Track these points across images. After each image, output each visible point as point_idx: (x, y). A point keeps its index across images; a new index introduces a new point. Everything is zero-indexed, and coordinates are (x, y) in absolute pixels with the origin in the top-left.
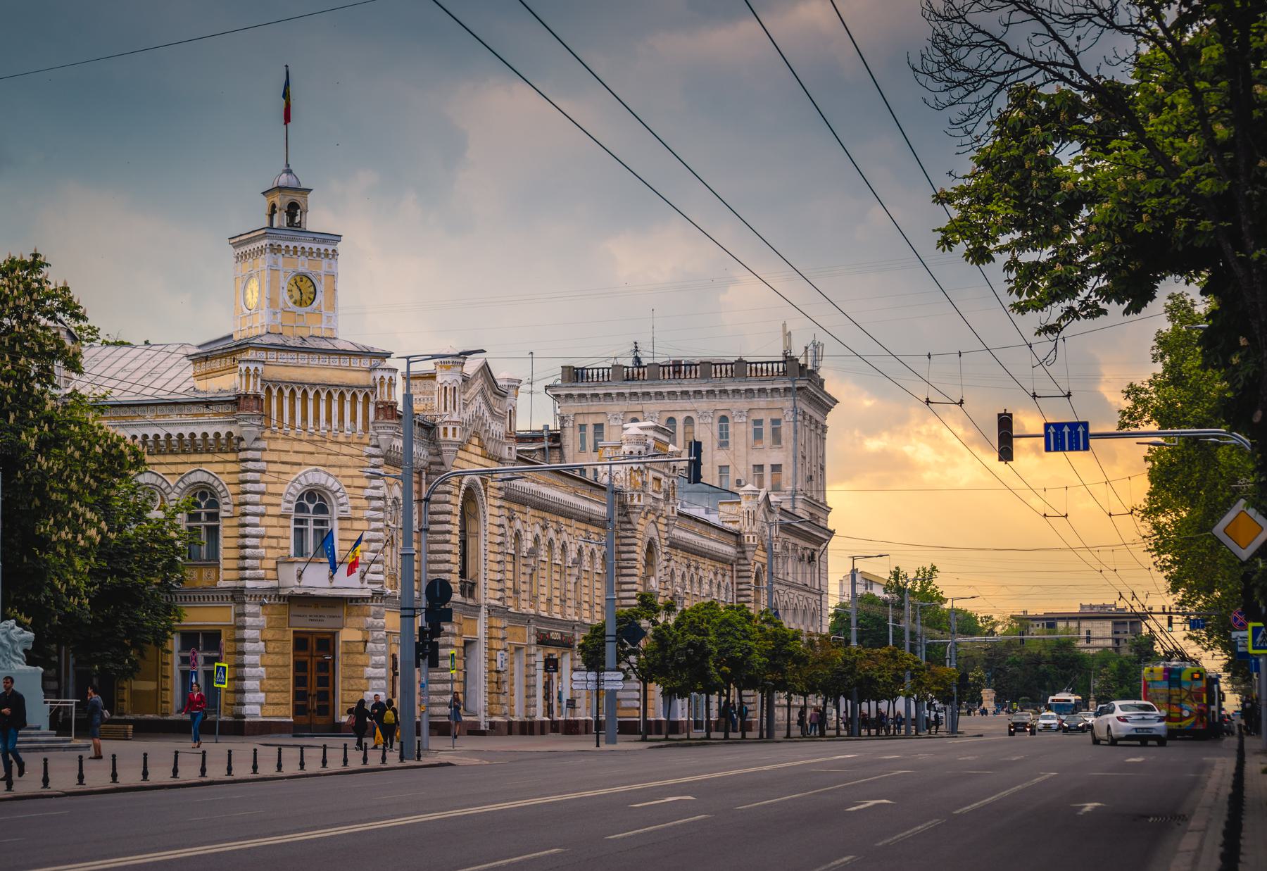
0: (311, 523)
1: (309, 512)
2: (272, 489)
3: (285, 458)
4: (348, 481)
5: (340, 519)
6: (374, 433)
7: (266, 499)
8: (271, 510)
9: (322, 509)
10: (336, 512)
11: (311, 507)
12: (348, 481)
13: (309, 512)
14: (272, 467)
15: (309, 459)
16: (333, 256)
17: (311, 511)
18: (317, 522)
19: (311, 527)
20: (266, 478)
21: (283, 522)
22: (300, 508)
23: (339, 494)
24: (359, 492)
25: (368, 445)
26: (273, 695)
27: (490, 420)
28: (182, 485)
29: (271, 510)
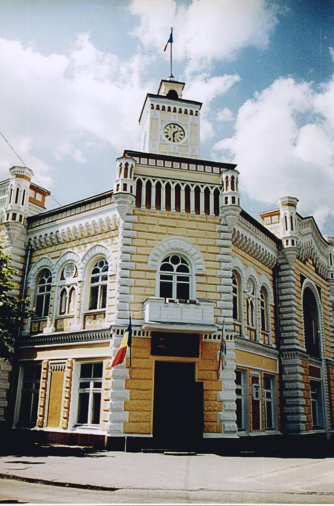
0: (175, 278)
1: (173, 270)
2: (140, 250)
3: (151, 229)
4: (204, 248)
5: (197, 275)
6: (223, 215)
7: (135, 258)
8: (139, 266)
9: (183, 269)
10: (193, 270)
11: (175, 267)
12: (204, 248)
13: (173, 270)
14: (141, 235)
15: (171, 230)
16: (196, 115)
17: (175, 269)
18: (179, 278)
19: (175, 282)
20: (135, 242)
21: (149, 275)
22: (164, 267)
23: (195, 257)
24: (212, 257)
25: (220, 224)
26: (134, 413)
27: (319, 253)
28: (87, 258)
29: (139, 266)
